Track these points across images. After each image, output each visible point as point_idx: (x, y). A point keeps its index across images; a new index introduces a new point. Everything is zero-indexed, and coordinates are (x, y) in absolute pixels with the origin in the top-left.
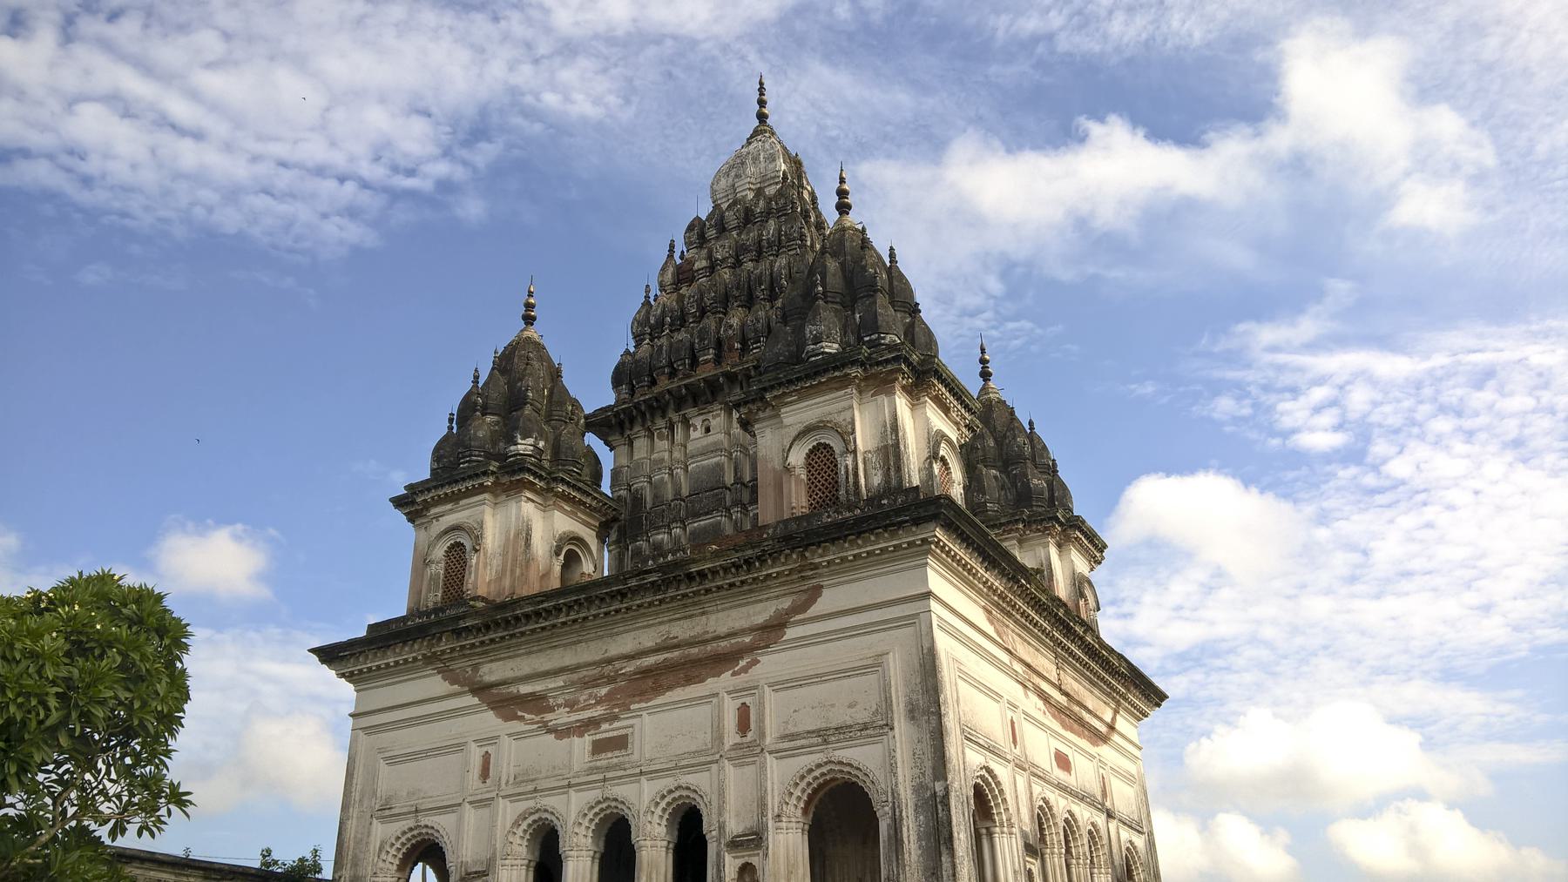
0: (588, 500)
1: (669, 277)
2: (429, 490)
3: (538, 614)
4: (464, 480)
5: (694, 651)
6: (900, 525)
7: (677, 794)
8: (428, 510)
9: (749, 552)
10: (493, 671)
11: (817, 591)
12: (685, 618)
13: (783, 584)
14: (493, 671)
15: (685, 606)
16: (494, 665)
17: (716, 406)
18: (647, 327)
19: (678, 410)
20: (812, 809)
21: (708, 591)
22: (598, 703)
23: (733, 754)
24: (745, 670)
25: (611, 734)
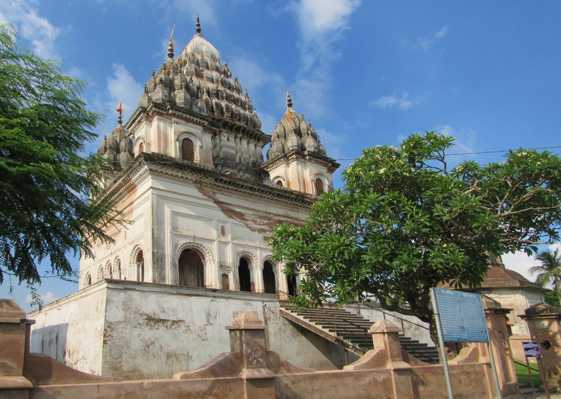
2: (180, 111)
10: (221, 197)
14: (221, 197)
16: (223, 196)
22: (264, 224)
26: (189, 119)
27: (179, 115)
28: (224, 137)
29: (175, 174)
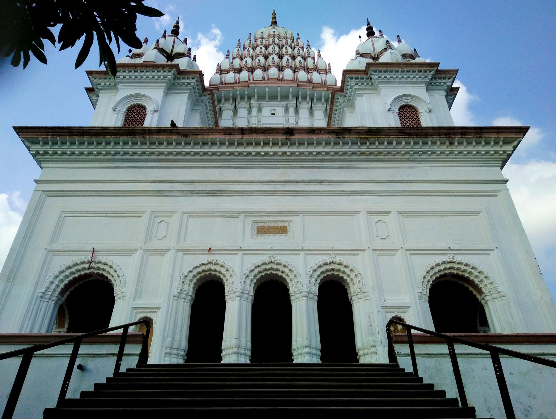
7: (330, 267)
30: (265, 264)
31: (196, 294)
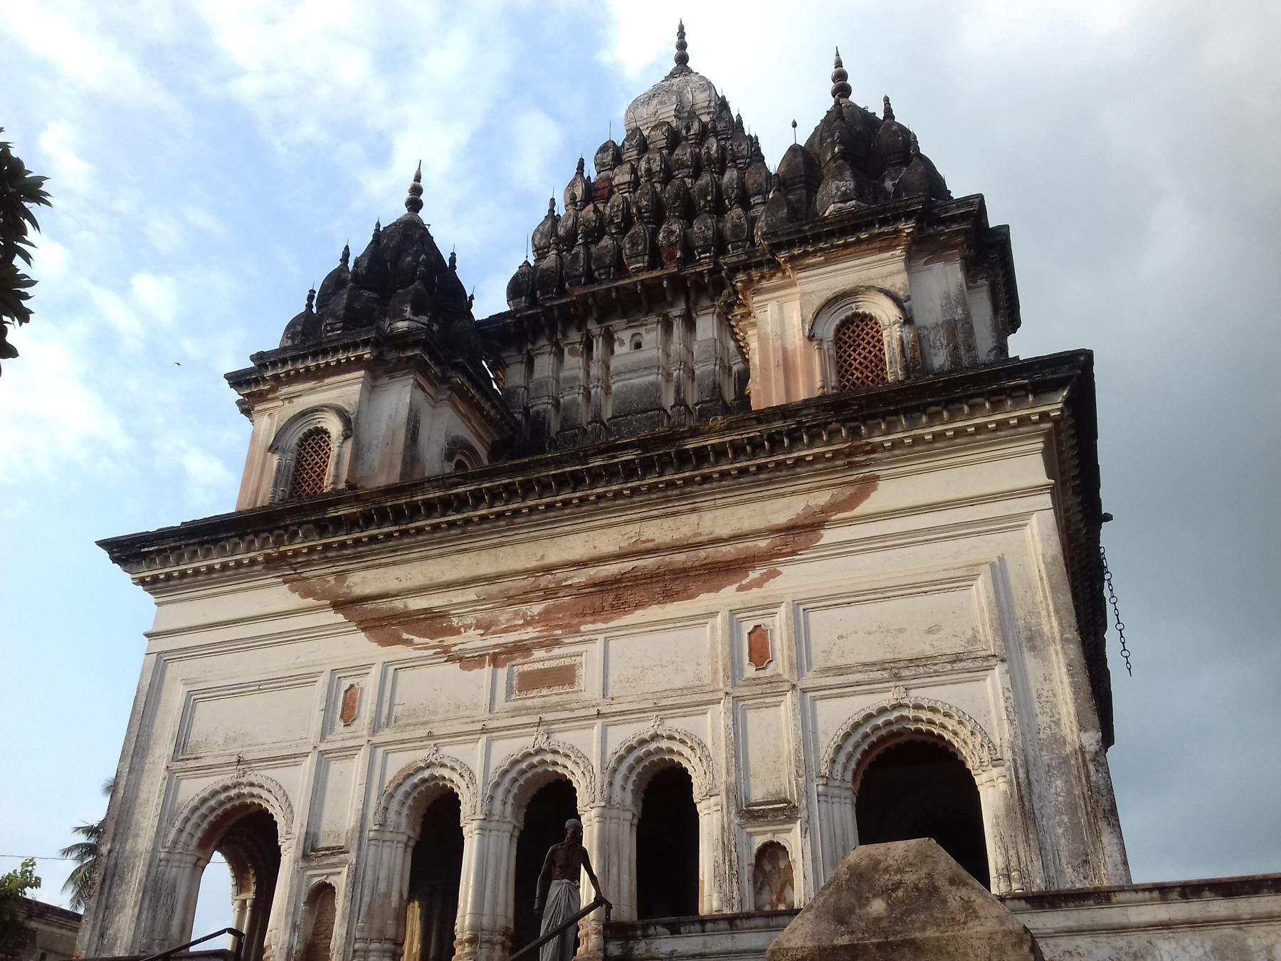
0: (487, 406)
1: (579, 192)
2: (284, 362)
3: (446, 505)
4: (335, 350)
5: (680, 558)
6: (1011, 392)
8: (274, 389)
9: (778, 424)
11: (869, 484)
12: (666, 515)
13: (818, 473)
14: (364, 581)
15: (668, 500)
16: (370, 574)
17: (653, 318)
18: (553, 236)
19: (600, 321)
20: (860, 777)
21: (706, 479)
22: (529, 622)
23: (744, 691)
24: (759, 583)
25: (547, 665)
26: (318, 366)
27: (287, 373)
28: (622, 343)
29: (202, 564)
30: (528, 755)
31: (424, 825)
